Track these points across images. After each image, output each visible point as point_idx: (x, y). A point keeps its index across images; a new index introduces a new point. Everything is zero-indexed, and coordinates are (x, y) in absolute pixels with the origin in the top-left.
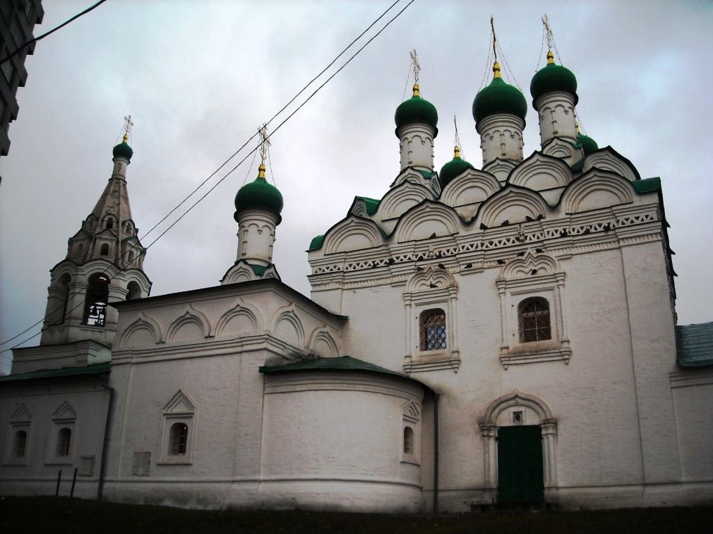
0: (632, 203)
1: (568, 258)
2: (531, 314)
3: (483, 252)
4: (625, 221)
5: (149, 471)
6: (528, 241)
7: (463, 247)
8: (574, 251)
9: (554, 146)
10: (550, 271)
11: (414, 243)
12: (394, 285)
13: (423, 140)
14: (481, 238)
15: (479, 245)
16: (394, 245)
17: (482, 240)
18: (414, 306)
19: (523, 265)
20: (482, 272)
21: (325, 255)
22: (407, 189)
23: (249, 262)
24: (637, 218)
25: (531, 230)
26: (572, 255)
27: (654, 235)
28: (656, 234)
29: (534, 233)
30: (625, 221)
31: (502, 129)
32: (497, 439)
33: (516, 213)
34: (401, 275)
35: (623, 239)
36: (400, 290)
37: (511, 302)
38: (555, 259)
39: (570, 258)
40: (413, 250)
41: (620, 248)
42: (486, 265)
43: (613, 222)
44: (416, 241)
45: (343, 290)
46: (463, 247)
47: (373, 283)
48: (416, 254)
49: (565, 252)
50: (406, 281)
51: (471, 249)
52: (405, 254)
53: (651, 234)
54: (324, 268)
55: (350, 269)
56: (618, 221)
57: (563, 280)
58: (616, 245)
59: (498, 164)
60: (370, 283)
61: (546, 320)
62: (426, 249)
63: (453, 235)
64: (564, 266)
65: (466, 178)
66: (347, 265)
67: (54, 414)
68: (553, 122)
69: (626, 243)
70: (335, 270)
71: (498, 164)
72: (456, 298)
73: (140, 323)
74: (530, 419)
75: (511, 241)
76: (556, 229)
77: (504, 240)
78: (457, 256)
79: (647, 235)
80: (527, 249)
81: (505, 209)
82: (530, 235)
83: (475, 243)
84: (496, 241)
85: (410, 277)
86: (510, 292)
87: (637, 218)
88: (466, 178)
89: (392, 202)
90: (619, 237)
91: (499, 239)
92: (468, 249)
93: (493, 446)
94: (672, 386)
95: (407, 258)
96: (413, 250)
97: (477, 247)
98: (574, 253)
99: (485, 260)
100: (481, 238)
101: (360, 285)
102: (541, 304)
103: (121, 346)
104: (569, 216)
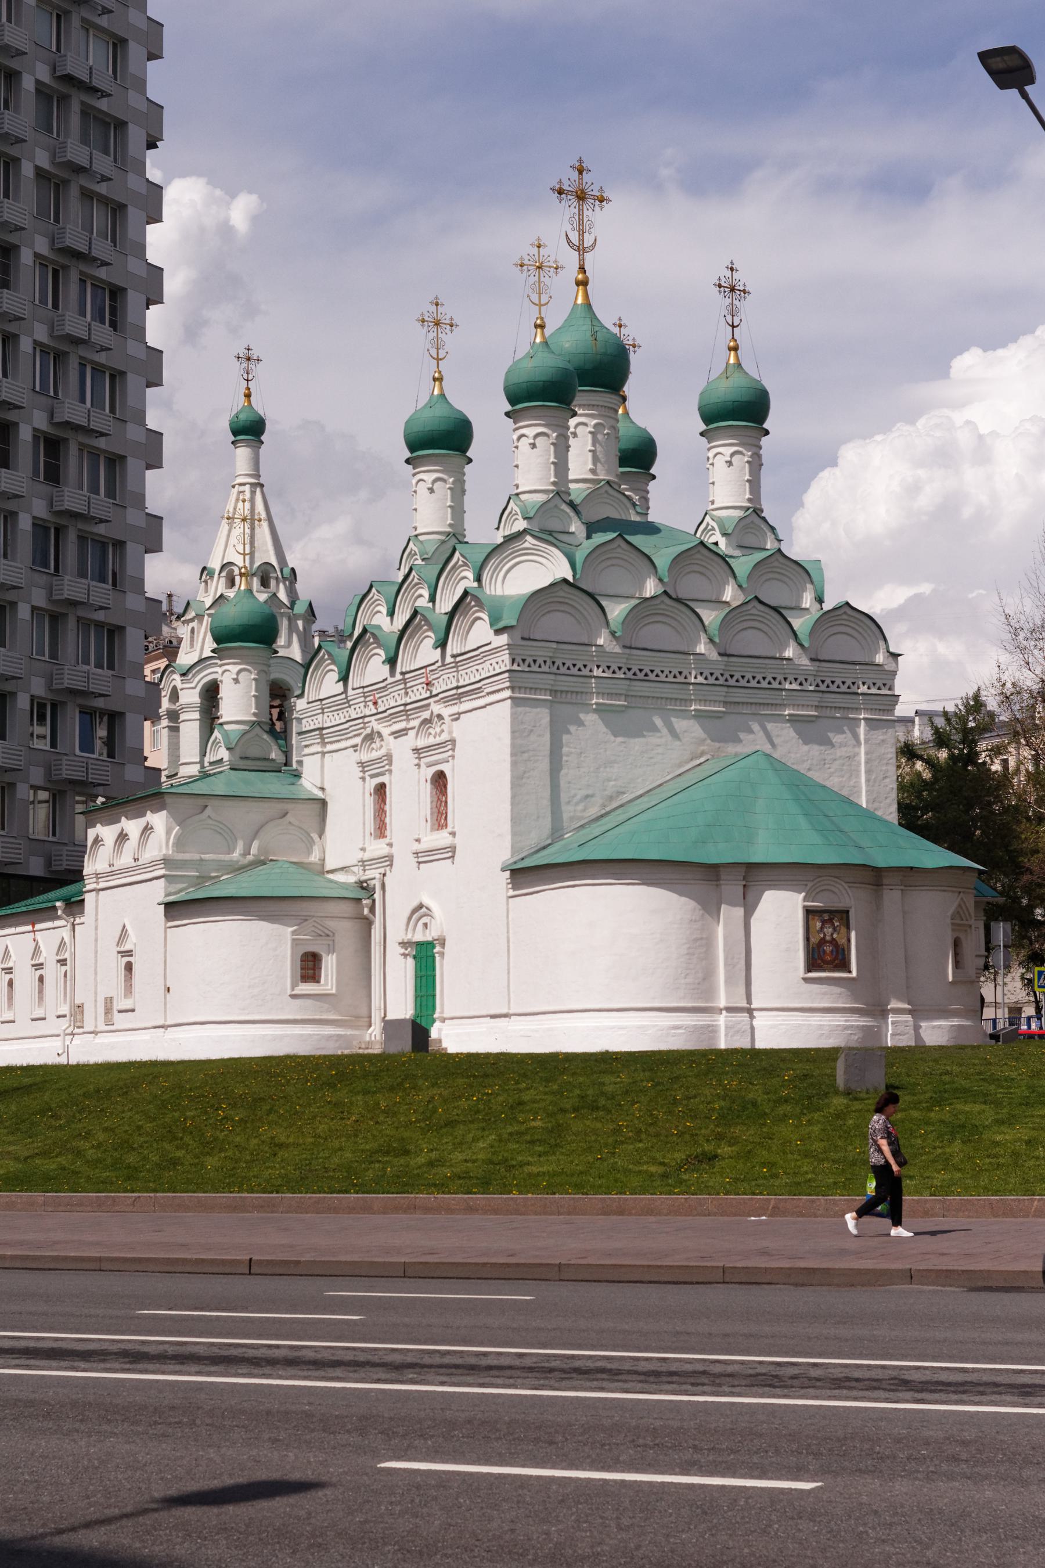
0: (490, 643)
1: (456, 717)
14: (402, 686)
16: (350, 692)
18: (368, 778)
20: (407, 734)
21: (308, 703)
22: (376, 597)
26: (459, 714)
28: (507, 688)
32: (415, 957)
36: (356, 757)
44: (363, 687)
45: (323, 754)
49: (455, 709)
80: (429, 705)
85: (358, 740)
86: (426, 764)
93: (410, 961)
96: (362, 699)
98: (461, 710)
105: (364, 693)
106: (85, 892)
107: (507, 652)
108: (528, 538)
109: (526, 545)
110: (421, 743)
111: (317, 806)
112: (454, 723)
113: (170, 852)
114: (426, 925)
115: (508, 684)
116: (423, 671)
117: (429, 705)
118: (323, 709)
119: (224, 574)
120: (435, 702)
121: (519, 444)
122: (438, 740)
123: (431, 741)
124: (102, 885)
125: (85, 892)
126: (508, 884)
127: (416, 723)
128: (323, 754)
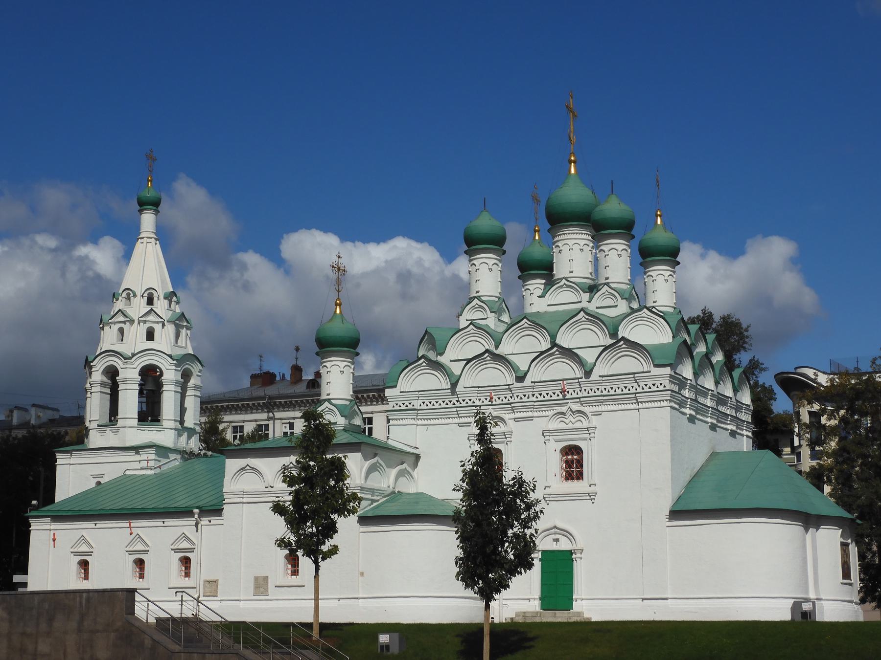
0: (650, 372)
1: (598, 414)
2: (570, 457)
3: (532, 403)
4: (644, 387)
5: (267, 591)
6: (568, 396)
7: (517, 396)
8: (604, 408)
9: (604, 293)
10: (586, 424)
11: (477, 389)
12: (460, 425)
13: (490, 267)
14: (532, 390)
15: (531, 396)
17: (533, 392)
19: (565, 417)
20: (532, 420)
21: (401, 392)
22: (472, 331)
23: (333, 402)
24: (654, 385)
25: (572, 387)
26: (602, 412)
27: (668, 401)
28: (666, 400)
29: (574, 389)
30: (644, 387)
31: (571, 242)
32: (540, 560)
33: (563, 369)
34: (466, 417)
35: (641, 402)
37: (555, 447)
38: (589, 415)
39: (601, 414)
40: (476, 394)
41: (638, 409)
42: (535, 414)
43: (636, 385)
44: (479, 387)
45: (417, 425)
46: (517, 396)
47: (444, 421)
48: (478, 398)
50: (471, 423)
51: (525, 399)
52: (470, 398)
53: (663, 401)
54: (400, 403)
55: (424, 407)
56: (639, 386)
57: (594, 433)
58: (635, 406)
59: (565, 284)
60: (440, 421)
61: (580, 463)
62: (489, 394)
63: (509, 385)
64: (595, 421)
65: (523, 327)
66: (420, 402)
67: (172, 545)
68: (606, 267)
69: (645, 405)
70: (410, 407)
71: (565, 284)
72: (511, 441)
73: (248, 467)
74: (564, 545)
75: (556, 394)
76: (591, 388)
77: (551, 393)
78: (513, 405)
79: (660, 401)
80: (568, 403)
81: (552, 364)
82: (571, 391)
83: (527, 394)
84: (544, 393)
87: (654, 385)
88: (523, 327)
89: (458, 343)
90: (639, 400)
91: (547, 392)
92: (521, 398)
94: (667, 525)
95: (472, 401)
97: (528, 398)
99: (535, 410)
100: (532, 390)
101: (432, 422)
102: (577, 450)
103: (232, 488)
104: (601, 378)
105: (478, 391)
106: (225, 504)
107: (669, 378)
108: (645, 310)
109: (644, 315)
110: (555, 425)
111: (413, 458)
112: (592, 416)
113: (363, 483)
114: (557, 540)
115: (669, 398)
116: (561, 382)
117: (568, 403)
118: (419, 397)
119: (146, 295)
120: (571, 403)
121: (609, 253)
122: (570, 426)
123: (562, 426)
124: (245, 500)
125: (225, 504)
126: (666, 518)
127: (550, 413)
128: (417, 425)
